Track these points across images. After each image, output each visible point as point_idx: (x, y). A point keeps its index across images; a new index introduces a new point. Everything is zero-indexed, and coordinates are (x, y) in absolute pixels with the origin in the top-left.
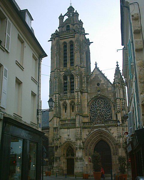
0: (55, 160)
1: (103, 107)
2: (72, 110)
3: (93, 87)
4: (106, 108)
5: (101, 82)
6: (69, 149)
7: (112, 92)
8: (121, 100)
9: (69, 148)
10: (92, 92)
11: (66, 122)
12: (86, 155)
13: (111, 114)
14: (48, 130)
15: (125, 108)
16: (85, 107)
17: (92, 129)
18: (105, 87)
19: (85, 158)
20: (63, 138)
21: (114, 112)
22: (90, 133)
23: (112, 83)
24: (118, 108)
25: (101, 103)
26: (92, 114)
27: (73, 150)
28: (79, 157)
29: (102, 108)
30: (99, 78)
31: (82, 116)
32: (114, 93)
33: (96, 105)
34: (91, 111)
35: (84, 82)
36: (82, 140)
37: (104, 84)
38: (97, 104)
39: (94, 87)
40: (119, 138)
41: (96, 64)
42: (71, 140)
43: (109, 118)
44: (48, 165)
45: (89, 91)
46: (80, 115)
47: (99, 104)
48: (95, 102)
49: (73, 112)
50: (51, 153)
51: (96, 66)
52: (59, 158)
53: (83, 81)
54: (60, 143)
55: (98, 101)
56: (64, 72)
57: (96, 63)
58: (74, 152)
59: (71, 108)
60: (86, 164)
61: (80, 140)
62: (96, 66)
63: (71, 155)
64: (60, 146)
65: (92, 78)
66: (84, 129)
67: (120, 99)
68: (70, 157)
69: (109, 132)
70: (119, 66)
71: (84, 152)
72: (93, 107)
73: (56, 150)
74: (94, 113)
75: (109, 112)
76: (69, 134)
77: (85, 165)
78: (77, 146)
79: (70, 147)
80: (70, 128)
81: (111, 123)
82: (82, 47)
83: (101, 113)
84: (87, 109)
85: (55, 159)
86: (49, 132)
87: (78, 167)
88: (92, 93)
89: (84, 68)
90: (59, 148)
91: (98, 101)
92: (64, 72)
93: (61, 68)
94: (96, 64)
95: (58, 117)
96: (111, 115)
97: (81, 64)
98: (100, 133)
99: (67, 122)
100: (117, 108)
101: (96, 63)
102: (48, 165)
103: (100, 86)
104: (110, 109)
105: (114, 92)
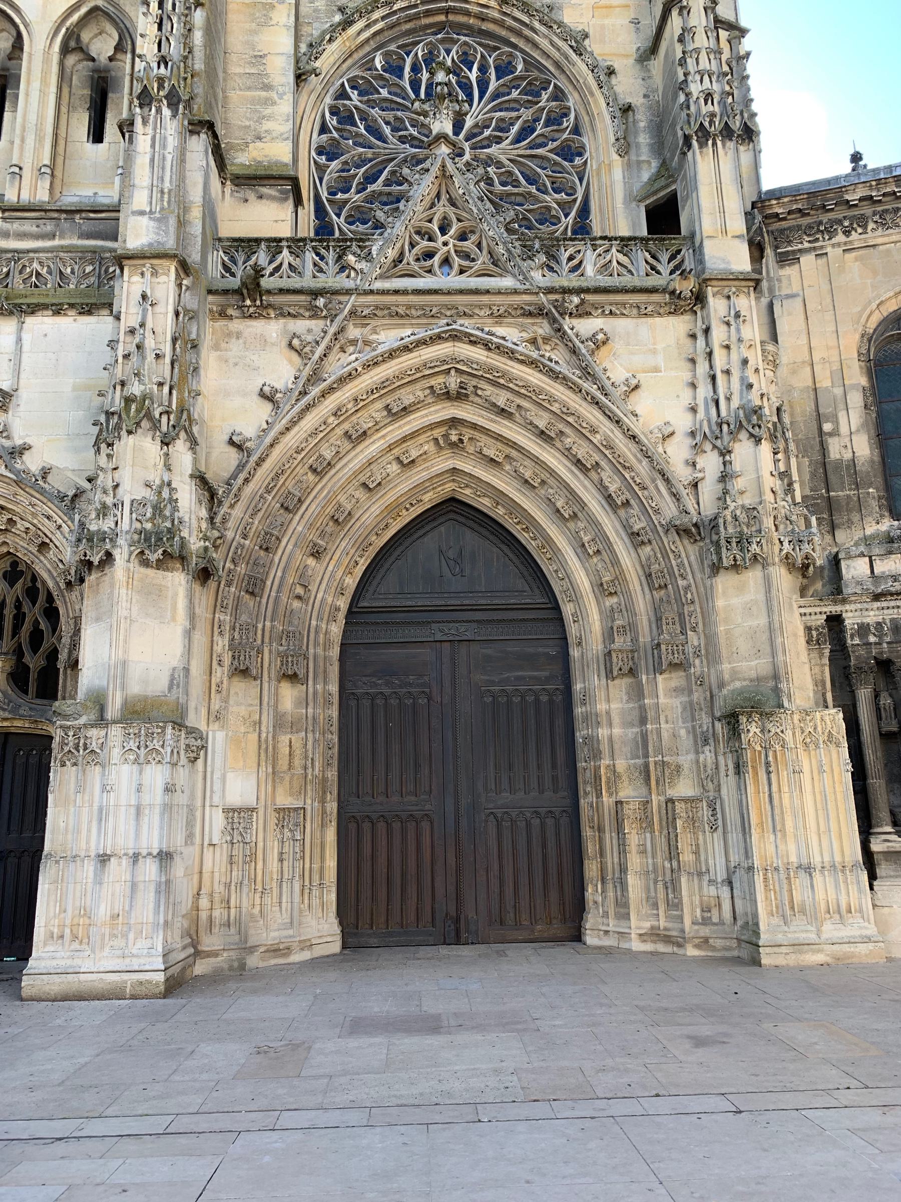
2: (81, 123)
4: (518, 140)
16: (267, 87)
17: (354, 332)
19: (217, 717)
21: (618, 173)
22: (315, 377)
24: (709, 96)
25: (466, 87)
28: (135, 689)
36: (193, 443)
40: (725, 453)
42: (32, 463)
49: (97, 136)
58: (66, 640)
59: (83, 92)
60: (230, 811)
66: (236, 325)
71: (215, 627)
74: (371, 178)
77: (218, 820)
78: (103, 511)
84: (285, 107)
87: (104, 859)
91: (430, 59)
96: (585, 211)
98: (453, 382)
100: (695, 88)
104: (570, 152)
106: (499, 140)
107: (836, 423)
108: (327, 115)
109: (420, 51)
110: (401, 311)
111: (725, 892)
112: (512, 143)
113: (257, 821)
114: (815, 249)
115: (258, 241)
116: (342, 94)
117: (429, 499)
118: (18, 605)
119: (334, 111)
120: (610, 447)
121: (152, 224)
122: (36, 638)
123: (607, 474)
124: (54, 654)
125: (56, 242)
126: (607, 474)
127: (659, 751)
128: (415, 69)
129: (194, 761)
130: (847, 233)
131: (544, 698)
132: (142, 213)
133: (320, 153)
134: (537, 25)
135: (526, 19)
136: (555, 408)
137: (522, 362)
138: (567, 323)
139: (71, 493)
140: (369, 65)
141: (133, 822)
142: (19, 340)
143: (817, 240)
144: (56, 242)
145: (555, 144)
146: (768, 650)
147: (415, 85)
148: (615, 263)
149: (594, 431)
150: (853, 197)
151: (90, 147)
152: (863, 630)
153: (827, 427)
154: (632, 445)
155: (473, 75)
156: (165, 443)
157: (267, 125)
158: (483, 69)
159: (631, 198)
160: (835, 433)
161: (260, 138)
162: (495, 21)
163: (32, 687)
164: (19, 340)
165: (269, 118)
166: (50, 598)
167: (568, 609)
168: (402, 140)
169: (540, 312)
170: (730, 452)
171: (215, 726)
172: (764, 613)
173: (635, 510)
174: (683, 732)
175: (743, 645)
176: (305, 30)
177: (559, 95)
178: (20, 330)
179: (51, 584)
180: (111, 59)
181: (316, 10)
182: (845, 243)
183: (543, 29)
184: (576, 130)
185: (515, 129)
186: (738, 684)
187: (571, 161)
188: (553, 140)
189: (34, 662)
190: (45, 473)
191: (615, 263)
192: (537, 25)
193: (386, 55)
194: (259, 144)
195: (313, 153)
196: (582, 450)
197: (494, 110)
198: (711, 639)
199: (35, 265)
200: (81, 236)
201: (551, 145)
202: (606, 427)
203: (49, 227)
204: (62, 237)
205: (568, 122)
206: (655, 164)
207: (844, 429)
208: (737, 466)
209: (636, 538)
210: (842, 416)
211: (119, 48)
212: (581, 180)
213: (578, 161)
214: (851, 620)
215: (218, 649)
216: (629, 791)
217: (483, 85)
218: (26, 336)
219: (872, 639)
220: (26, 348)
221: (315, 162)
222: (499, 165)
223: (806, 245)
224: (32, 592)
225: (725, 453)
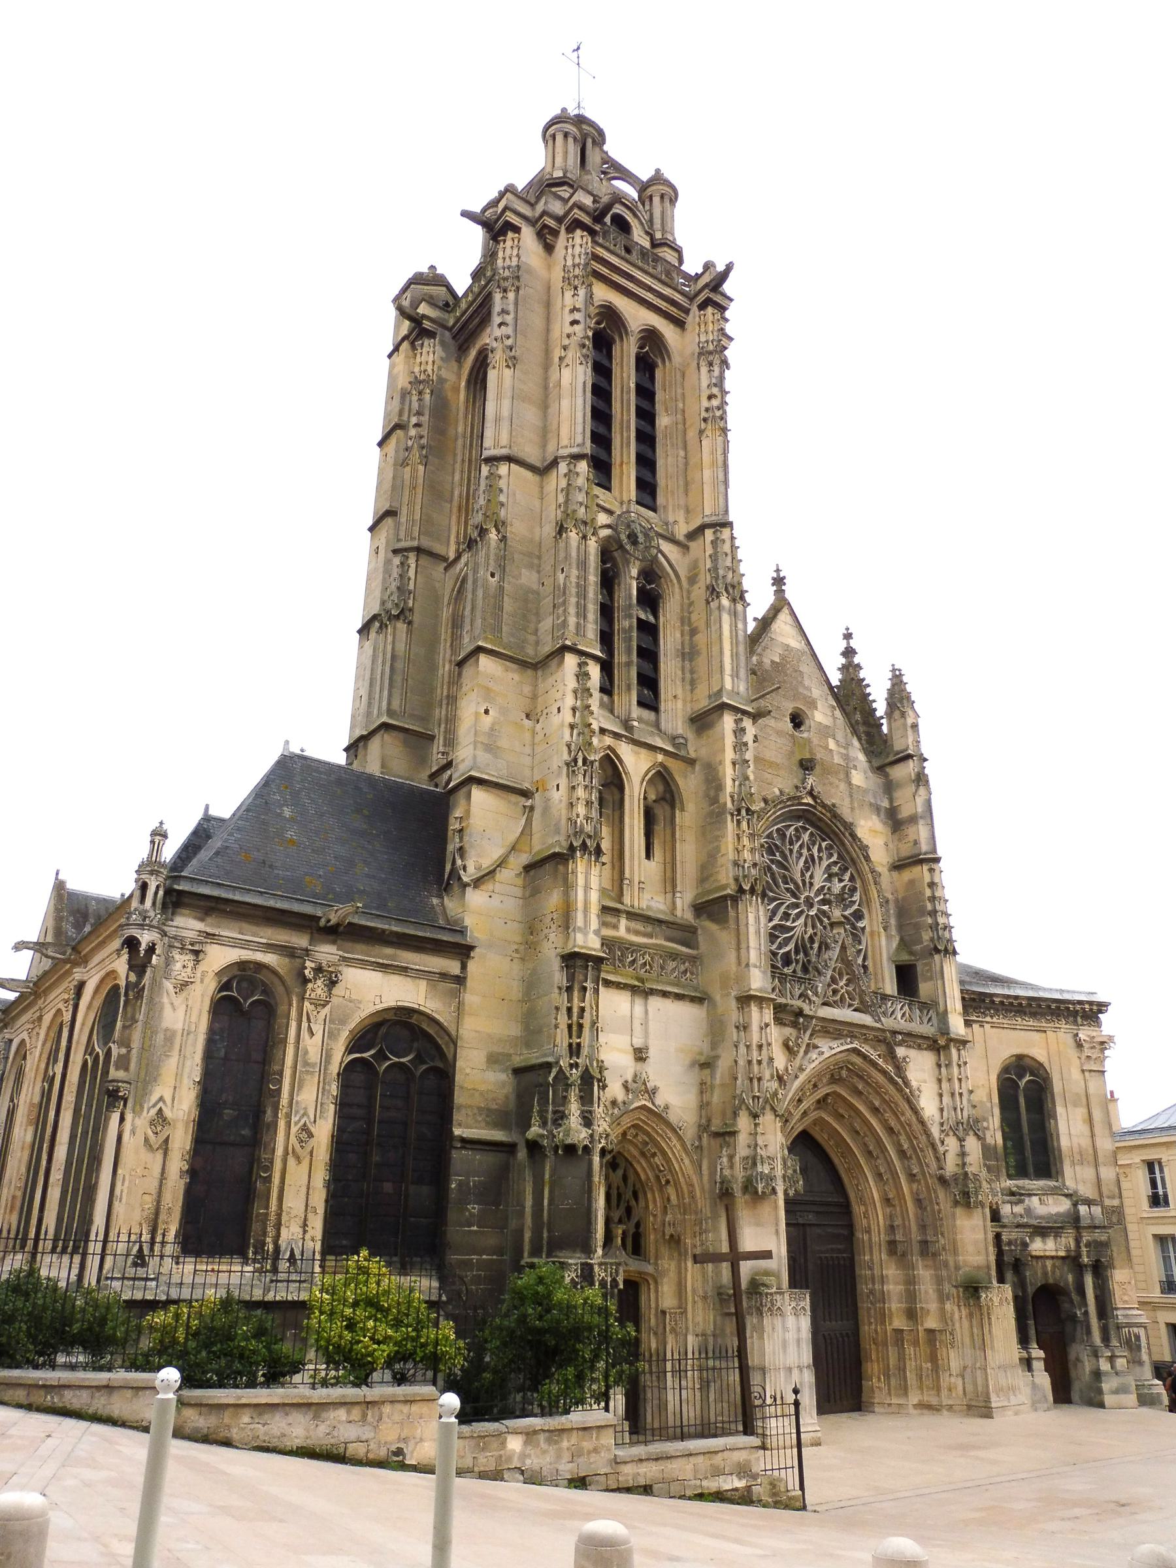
7: (871, 804)
11: (615, 927)
14: (454, 967)
18: (837, 760)
37: (826, 732)
40: (961, 1140)
41: (779, 581)
42: (660, 1100)
51: (780, 593)
62: (780, 593)
70: (856, 660)
76: (638, 1043)
80: (652, 992)
86: (460, 980)
94: (779, 581)
99: (628, 930)
107: (988, 1122)
110: (831, 1030)
111: (960, 1382)
114: (979, 1021)
120: (910, 1125)
123: (903, 1138)
126: (903, 1138)
127: (920, 1302)
131: (842, 1262)
132: (755, 966)
134: (847, 834)
135: (842, 829)
136: (887, 1097)
137: (879, 1071)
141: (796, 1349)
142: (646, 1012)
143: (978, 1017)
146: (984, 1252)
147: (791, 851)
149: (903, 1114)
150: (997, 1000)
152: (1010, 1243)
154: (920, 1126)
158: (820, 850)
159: (889, 959)
160: (987, 1128)
162: (827, 824)
164: (646, 1012)
167: (858, 1210)
168: (787, 890)
169: (883, 1041)
170: (964, 1140)
172: (983, 1231)
173: (914, 1161)
174: (931, 1291)
175: (971, 1248)
180: (654, 801)
183: (850, 838)
186: (967, 1269)
190: (667, 1107)
192: (847, 834)
196: (893, 1123)
198: (954, 1243)
199: (647, 957)
202: (909, 1113)
203: (649, 929)
204: (656, 938)
206: (898, 939)
207: (991, 1127)
208: (967, 1149)
209: (912, 1177)
210: (990, 1118)
214: (1004, 1238)
216: (899, 1322)
218: (650, 1009)
219: (1013, 1247)
223: (975, 1018)
225: (961, 1140)
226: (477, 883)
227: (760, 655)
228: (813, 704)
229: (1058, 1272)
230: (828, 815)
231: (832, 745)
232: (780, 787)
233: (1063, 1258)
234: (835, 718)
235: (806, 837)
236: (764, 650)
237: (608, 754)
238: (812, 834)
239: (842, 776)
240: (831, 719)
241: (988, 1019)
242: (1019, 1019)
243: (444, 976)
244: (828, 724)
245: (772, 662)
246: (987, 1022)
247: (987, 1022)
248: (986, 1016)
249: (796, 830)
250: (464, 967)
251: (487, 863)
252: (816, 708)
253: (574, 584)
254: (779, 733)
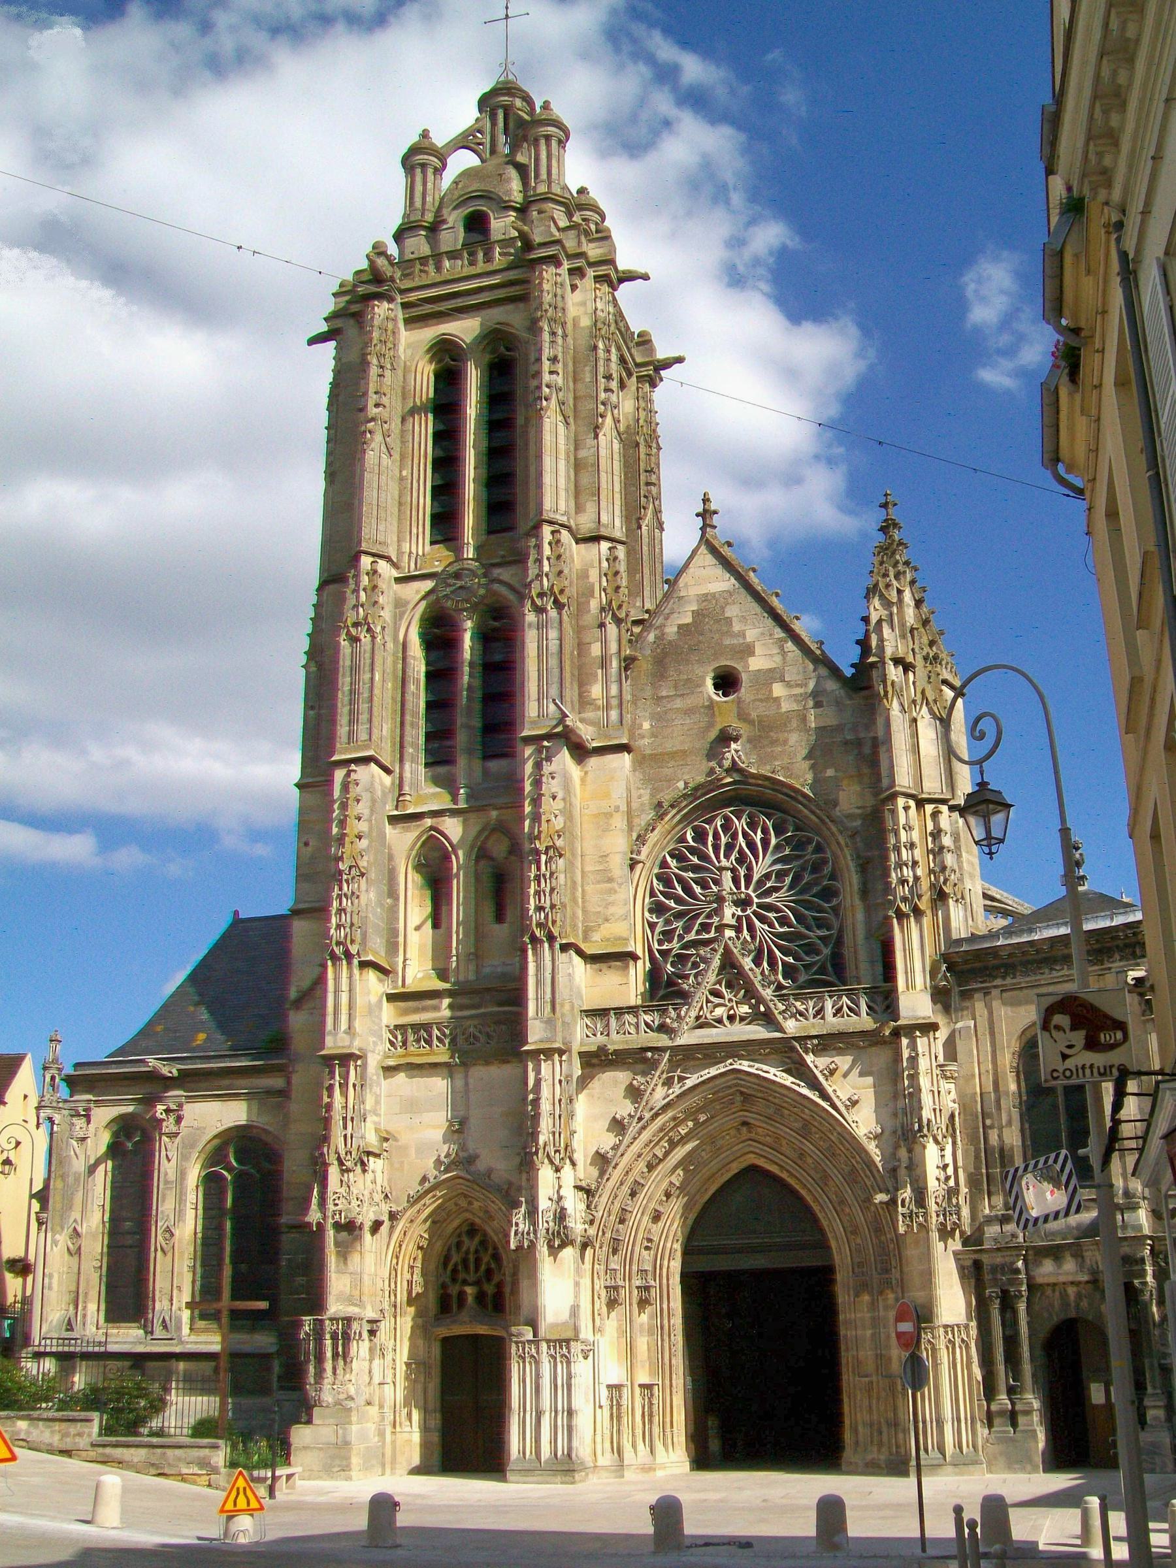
0: (328, 1343)
1: (767, 876)
3: (678, 703)
5: (757, 663)
6: (459, 1245)
7: (846, 743)
8: (929, 808)
9: (465, 1239)
10: (670, 746)
12: (612, 1304)
13: (841, 931)
14: (277, 1082)
15: (961, 880)
16: (610, 880)
18: (785, 706)
20: (404, 1149)
21: (860, 916)
23: (849, 672)
25: (751, 845)
26: (668, 935)
27: (496, 1257)
29: (760, 883)
30: (736, 627)
31: (580, 953)
32: (867, 750)
33: (704, 857)
34: (658, 909)
35: (604, 662)
38: (716, 848)
39: (689, 702)
41: (706, 515)
42: (481, 1165)
43: (822, 970)
44: (275, 1385)
45: (646, 741)
46: (565, 948)
47: (730, 847)
48: (700, 836)
50: (301, 1280)
52: (366, 1327)
53: (596, 650)
54: (378, 1197)
55: (727, 826)
56: (429, 585)
57: (706, 500)
61: (557, 1170)
63: (480, 1297)
64: (376, 1226)
65: (671, 630)
67: (920, 803)
68: (466, 1326)
69: (824, 1096)
72: (680, 880)
73: (344, 1253)
75: (821, 924)
79: (472, 1231)
81: (838, 1012)
82: (588, 378)
83: (751, 928)
85: (334, 1337)
86: (284, 1093)
88: (673, 755)
89: (604, 545)
90: (367, 1236)
91: (727, 826)
92: (429, 585)
93: (406, 547)
95: (364, 965)
96: (839, 942)
97: (579, 509)
101: (706, 500)
102: (275, 1385)
103: (745, 692)
104: (828, 894)
105: (859, 743)
106: (776, 889)
108: (655, 881)
109: (719, 822)
112: (788, 890)
113: (626, 1393)
115: (609, 1009)
116: (664, 864)
117: (735, 1168)
118: (477, 1251)
119: (659, 877)
121: (543, 1025)
122: (489, 1273)
124: (500, 1286)
125: (482, 1010)
128: (716, 836)
129: (586, 1358)
130: (1004, 978)
133: (651, 911)
138: (809, 1059)
139: (506, 1187)
140: (682, 839)
142: (467, 1084)
144: (482, 1010)
145: (819, 888)
148: (845, 1008)
151: (497, 927)
153: (988, 1122)
155: (758, 837)
156: (557, 1170)
157: (612, 910)
158: (765, 831)
160: (992, 1127)
161: (607, 920)
163: (490, 1307)
164: (467, 1084)
165: (612, 904)
166: (495, 1248)
171: (598, 1336)
176: (636, 821)
177: (819, 849)
178: (466, 1077)
179: (496, 1239)
181: (642, 804)
182: (1002, 986)
184: (833, 877)
185: (788, 880)
187: (828, 902)
188: (816, 884)
189: (490, 1289)
191: (845, 1008)
193: (694, 829)
194: (607, 925)
195: (647, 914)
197: (775, 862)
200: (500, 1004)
201: (815, 890)
203: (477, 1000)
205: (827, 870)
211: (511, 852)
212: (837, 915)
213: (835, 902)
215: (597, 1287)
217: (765, 842)
218: (471, 1081)
220: (471, 1086)
221: (648, 922)
222: (778, 910)
224: (484, 1243)
226: (298, 1003)
227: (662, 626)
228: (749, 650)
229: (1084, 1304)
230: (766, 783)
231: (778, 690)
232: (686, 777)
233: (1087, 1282)
234: (783, 653)
235: (740, 825)
236: (666, 619)
237: (432, 836)
238: (750, 816)
239: (794, 724)
240: (778, 659)
241: (998, 982)
242: (1047, 971)
243: (269, 1092)
244: (773, 665)
245: (680, 627)
246: (995, 987)
247: (995, 987)
248: (995, 977)
249: (727, 819)
250: (289, 1083)
251: (306, 984)
252: (752, 654)
253: (347, 693)
254: (688, 712)
